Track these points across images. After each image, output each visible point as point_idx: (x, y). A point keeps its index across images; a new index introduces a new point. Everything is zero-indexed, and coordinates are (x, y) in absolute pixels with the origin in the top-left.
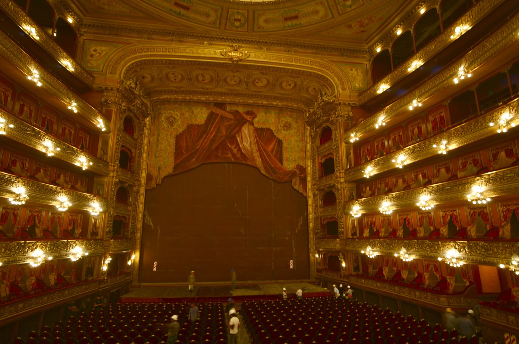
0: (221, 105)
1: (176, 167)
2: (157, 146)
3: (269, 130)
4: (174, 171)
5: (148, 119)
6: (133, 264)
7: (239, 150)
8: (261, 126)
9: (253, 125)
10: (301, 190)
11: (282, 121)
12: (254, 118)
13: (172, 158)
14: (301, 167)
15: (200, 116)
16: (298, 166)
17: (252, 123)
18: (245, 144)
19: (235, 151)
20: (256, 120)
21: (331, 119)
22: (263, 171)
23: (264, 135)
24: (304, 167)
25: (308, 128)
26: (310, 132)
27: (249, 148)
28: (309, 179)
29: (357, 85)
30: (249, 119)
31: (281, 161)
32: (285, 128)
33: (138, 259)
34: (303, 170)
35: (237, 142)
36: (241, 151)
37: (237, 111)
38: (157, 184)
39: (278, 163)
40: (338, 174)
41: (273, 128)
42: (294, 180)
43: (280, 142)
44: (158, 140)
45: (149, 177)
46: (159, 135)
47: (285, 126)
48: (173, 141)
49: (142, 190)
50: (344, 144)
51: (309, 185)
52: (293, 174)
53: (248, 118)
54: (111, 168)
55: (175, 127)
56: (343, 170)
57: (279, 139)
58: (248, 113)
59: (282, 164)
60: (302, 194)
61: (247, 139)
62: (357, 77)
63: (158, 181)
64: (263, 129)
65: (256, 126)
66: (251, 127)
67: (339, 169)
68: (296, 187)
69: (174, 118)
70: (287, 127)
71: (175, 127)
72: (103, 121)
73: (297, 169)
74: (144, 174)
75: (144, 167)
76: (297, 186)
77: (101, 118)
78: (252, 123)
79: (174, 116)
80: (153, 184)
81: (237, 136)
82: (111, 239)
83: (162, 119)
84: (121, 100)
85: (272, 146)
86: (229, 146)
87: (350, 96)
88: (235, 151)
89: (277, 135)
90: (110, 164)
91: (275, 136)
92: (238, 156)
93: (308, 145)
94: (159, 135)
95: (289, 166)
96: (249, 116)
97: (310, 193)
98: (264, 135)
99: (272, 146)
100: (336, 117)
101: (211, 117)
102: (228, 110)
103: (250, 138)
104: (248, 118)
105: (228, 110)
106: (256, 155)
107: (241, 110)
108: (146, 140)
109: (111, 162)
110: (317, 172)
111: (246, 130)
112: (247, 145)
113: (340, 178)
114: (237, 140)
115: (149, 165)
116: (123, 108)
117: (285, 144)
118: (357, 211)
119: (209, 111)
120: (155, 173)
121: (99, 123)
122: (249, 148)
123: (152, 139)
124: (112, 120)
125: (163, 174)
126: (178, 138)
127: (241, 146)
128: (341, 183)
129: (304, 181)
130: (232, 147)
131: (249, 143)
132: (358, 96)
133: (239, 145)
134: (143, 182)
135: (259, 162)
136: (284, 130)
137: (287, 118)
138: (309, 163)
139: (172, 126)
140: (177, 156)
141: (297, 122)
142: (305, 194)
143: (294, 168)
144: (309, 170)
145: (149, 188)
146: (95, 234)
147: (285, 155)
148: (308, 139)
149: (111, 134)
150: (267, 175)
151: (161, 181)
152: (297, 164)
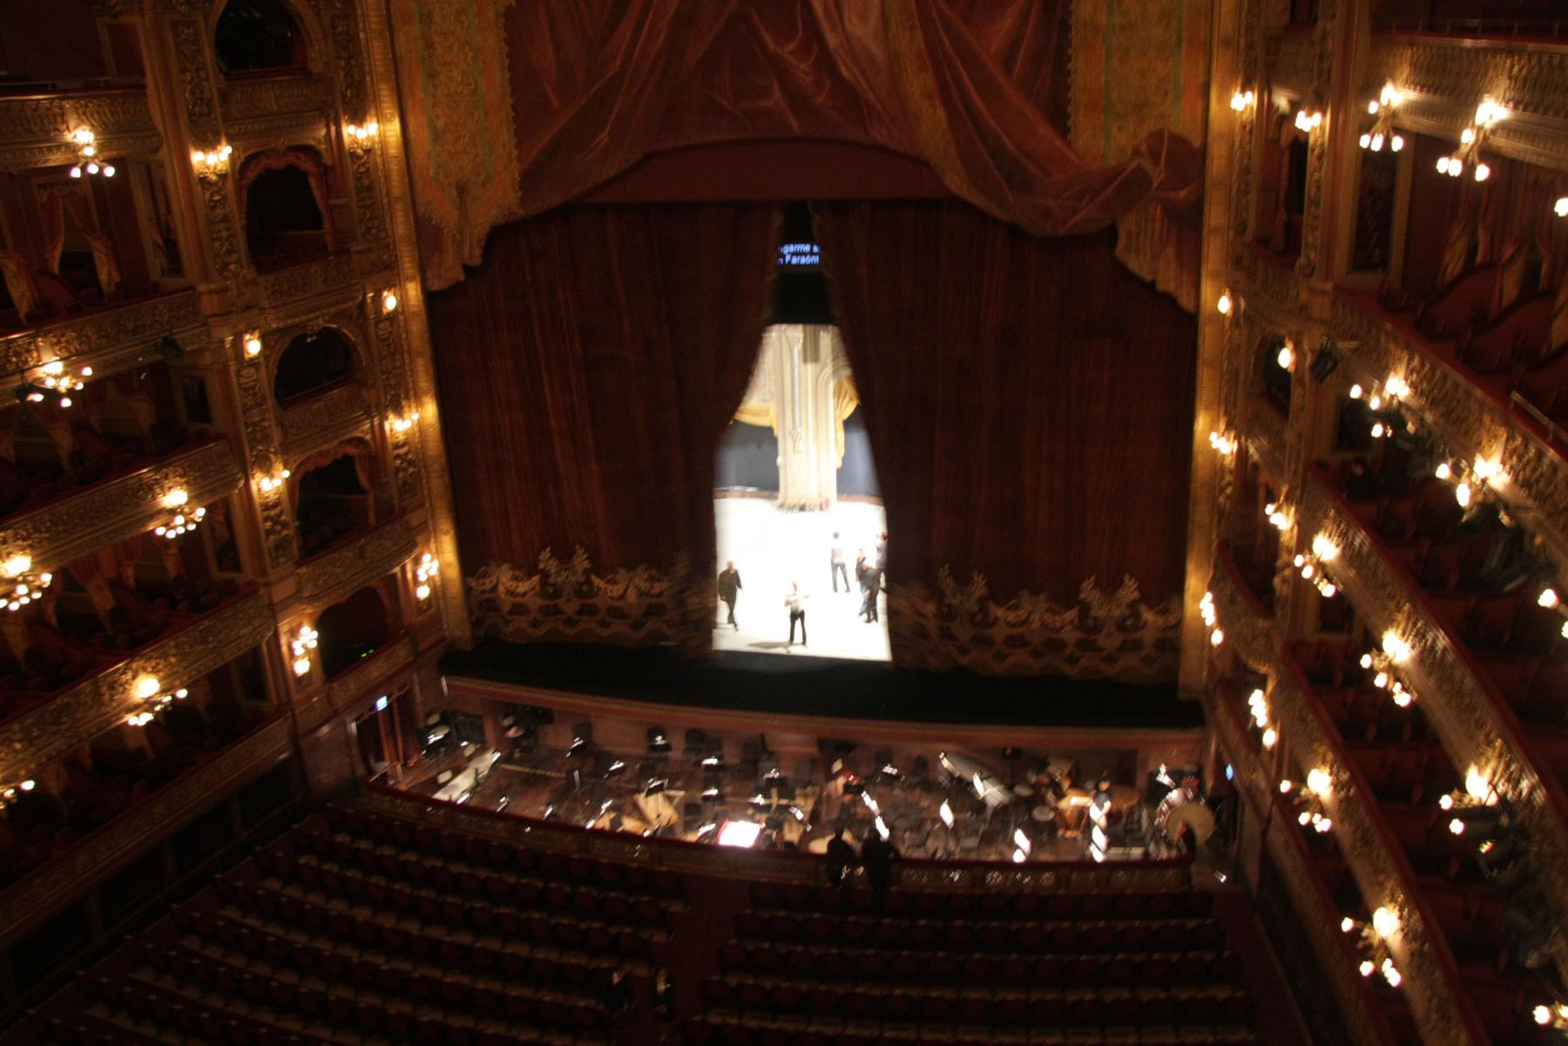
1: (529, 181)
2: (432, 75)
4: (523, 202)
6: (439, 589)
7: (825, 62)
10: (1168, 280)
13: (506, 137)
14: (1178, 141)
16: (1160, 133)
19: (803, 70)
22: (956, 182)
24: (1197, 143)
27: (878, 51)
28: (1215, 215)
31: (1059, 118)
33: (454, 573)
36: (833, 70)
38: (467, 269)
39: (1045, 130)
40: (1304, 296)
44: (430, 45)
45: (427, 237)
46: (427, 19)
48: (492, 42)
52: (1129, 187)
60: (1169, 300)
68: (1138, 264)
73: (1155, 156)
74: (401, 225)
75: (396, 192)
80: (450, 272)
85: (1005, 25)
86: (771, 44)
88: (803, 70)
90: (201, 288)
92: (819, 99)
94: (429, 15)
95: (1104, 141)
99: (1005, 25)
106: (918, 85)
109: (206, 279)
110: (1253, 196)
112: (862, 29)
115: (416, 176)
120: (444, 211)
122: (878, 51)
123: (401, 39)
125: (484, 217)
127: (832, 40)
129: (1186, 225)
131: (876, 12)
133: (819, 37)
135: (931, 127)
140: (524, 126)
142: (1185, 302)
143: (1136, 152)
145: (436, 285)
147: (1085, 72)
149: (164, 151)
150: (977, 199)
151: (478, 252)
152: (1151, 125)
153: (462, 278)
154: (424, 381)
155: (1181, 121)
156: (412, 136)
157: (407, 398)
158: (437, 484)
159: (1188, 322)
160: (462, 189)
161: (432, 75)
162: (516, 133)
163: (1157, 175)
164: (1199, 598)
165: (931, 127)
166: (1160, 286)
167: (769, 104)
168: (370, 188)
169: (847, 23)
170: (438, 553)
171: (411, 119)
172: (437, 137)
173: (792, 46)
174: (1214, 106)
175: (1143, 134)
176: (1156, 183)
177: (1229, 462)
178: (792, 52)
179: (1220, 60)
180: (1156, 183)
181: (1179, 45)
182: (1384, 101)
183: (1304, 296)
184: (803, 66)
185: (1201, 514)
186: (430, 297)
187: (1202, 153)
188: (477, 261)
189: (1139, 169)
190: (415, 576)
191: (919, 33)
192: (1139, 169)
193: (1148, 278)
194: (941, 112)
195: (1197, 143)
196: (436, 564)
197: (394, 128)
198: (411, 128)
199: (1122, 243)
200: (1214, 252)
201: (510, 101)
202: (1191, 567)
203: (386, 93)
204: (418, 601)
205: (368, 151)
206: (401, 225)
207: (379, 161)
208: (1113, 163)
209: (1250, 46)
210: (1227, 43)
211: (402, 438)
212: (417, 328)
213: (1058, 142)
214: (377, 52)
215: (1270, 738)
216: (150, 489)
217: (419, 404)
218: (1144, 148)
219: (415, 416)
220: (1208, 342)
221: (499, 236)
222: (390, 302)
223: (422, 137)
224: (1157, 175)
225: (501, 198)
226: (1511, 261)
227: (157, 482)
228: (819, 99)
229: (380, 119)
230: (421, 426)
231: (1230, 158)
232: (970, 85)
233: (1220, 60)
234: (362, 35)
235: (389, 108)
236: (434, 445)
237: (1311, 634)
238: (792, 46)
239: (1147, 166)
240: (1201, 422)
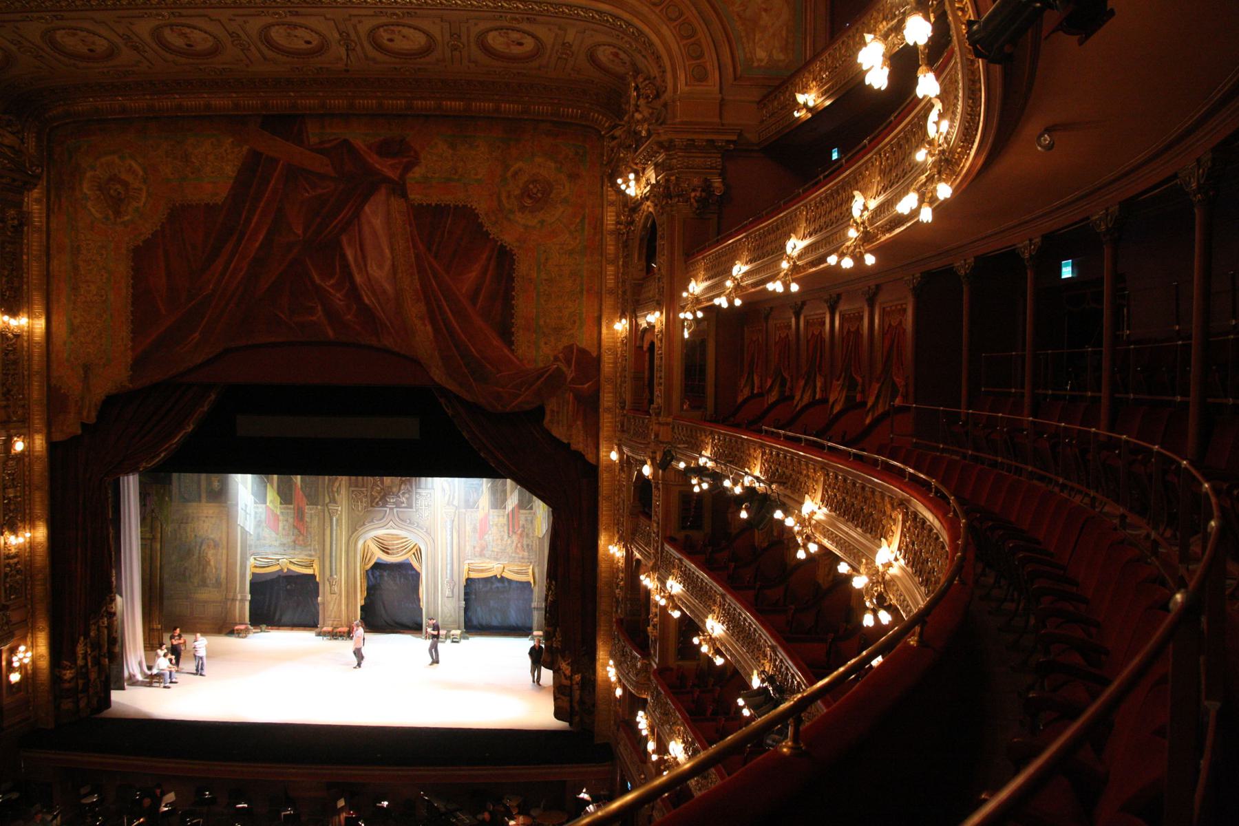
0: (285, 124)
2: (75, 289)
3: (466, 214)
7: (354, 293)
8: (434, 200)
10: (578, 443)
11: (515, 175)
12: (408, 168)
14: (582, 352)
15: (213, 169)
16: (569, 349)
17: (399, 189)
18: (374, 270)
19: (338, 299)
20: (417, 173)
22: (438, 375)
23: (446, 233)
24: (595, 355)
28: (607, 399)
29: (761, 54)
31: (506, 334)
32: (528, 202)
35: (345, 265)
36: (359, 299)
37: (345, 140)
38: (84, 426)
41: (481, 205)
42: (551, 405)
43: (504, 258)
44: (76, 268)
45: (56, 402)
47: (526, 193)
53: (386, 167)
55: (126, 218)
58: (384, 149)
59: (510, 344)
60: (580, 456)
61: (380, 251)
62: (765, 19)
63: (85, 414)
64: (440, 211)
65: (416, 197)
66: (397, 204)
68: (558, 432)
69: (125, 184)
70: (537, 196)
71: (126, 218)
73: (568, 362)
74: (36, 391)
75: (36, 368)
76: (562, 427)
78: (399, 189)
79: (124, 176)
80: (71, 426)
81: (344, 239)
83: (85, 190)
86: (317, 280)
87: (722, 103)
89: (494, 231)
91: (487, 234)
93: (611, 269)
95: (536, 351)
96: (391, 162)
101: (253, 171)
102: (314, 140)
103: (392, 250)
104: (386, 167)
105: (314, 140)
106: (415, 310)
107: (360, 137)
112: (379, 272)
114: (343, 257)
115: (53, 356)
117: (523, 267)
119: (245, 148)
122: (388, 287)
125: (103, 387)
126: (141, 256)
127: (358, 279)
129: (589, 407)
130: (328, 284)
131: (389, 263)
132: (761, 103)
133: (350, 276)
135: (423, 338)
136: (523, 208)
137: (538, 160)
139: (118, 213)
141: (573, 177)
142: (590, 458)
143: (556, 359)
145: (58, 437)
147: (523, 306)
150: (451, 386)
151: (94, 414)
152: (565, 341)
153: (80, 432)
154: (39, 509)
155: (584, 340)
156: (54, 329)
157: (23, 521)
158: (40, 589)
159: (592, 470)
160: (87, 368)
161: (75, 289)
162: (133, 332)
163: (570, 374)
164: (606, 665)
165: (423, 338)
166: (574, 447)
167: (314, 318)
168: (15, 362)
169: (369, 269)
170: (33, 646)
171: (54, 317)
172: (73, 331)
174: (604, 331)
175: (561, 348)
177: (622, 563)
178: (332, 286)
179: (608, 302)
181: (581, 292)
182: (691, 290)
183: (655, 427)
185: (603, 605)
186: (52, 446)
187: (598, 360)
188: (93, 419)
189: (558, 369)
192: (558, 369)
193: (565, 441)
194: (429, 328)
195: (595, 355)
197: (40, 325)
198: (54, 324)
199: (548, 418)
200: (607, 422)
201: (130, 308)
202: (600, 643)
203: (37, 298)
205: (17, 336)
207: (25, 344)
208: (541, 365)
209: (624, 293)
210: (611, 292)
211: (13, 551)
212: (39, 468)
213: (506, 351)
214: (35, 271)
217: (33, 527)
218: (561, 356)
219: (28, 535)
220: (605, 482)
221: (110, 403)
222: (19, 446)
223: (61, 330)
224: (570, 374)
225: (115, 375)
226: (771, 386)
229: (31, 315)
230: (32, 544)
231: (615, 363)
232: (450, 314)
233: (608, 302)
234: (25, 257)
235: (38, 308)
237: (673, 662)
239: (564, 369)
240: (602, 540)
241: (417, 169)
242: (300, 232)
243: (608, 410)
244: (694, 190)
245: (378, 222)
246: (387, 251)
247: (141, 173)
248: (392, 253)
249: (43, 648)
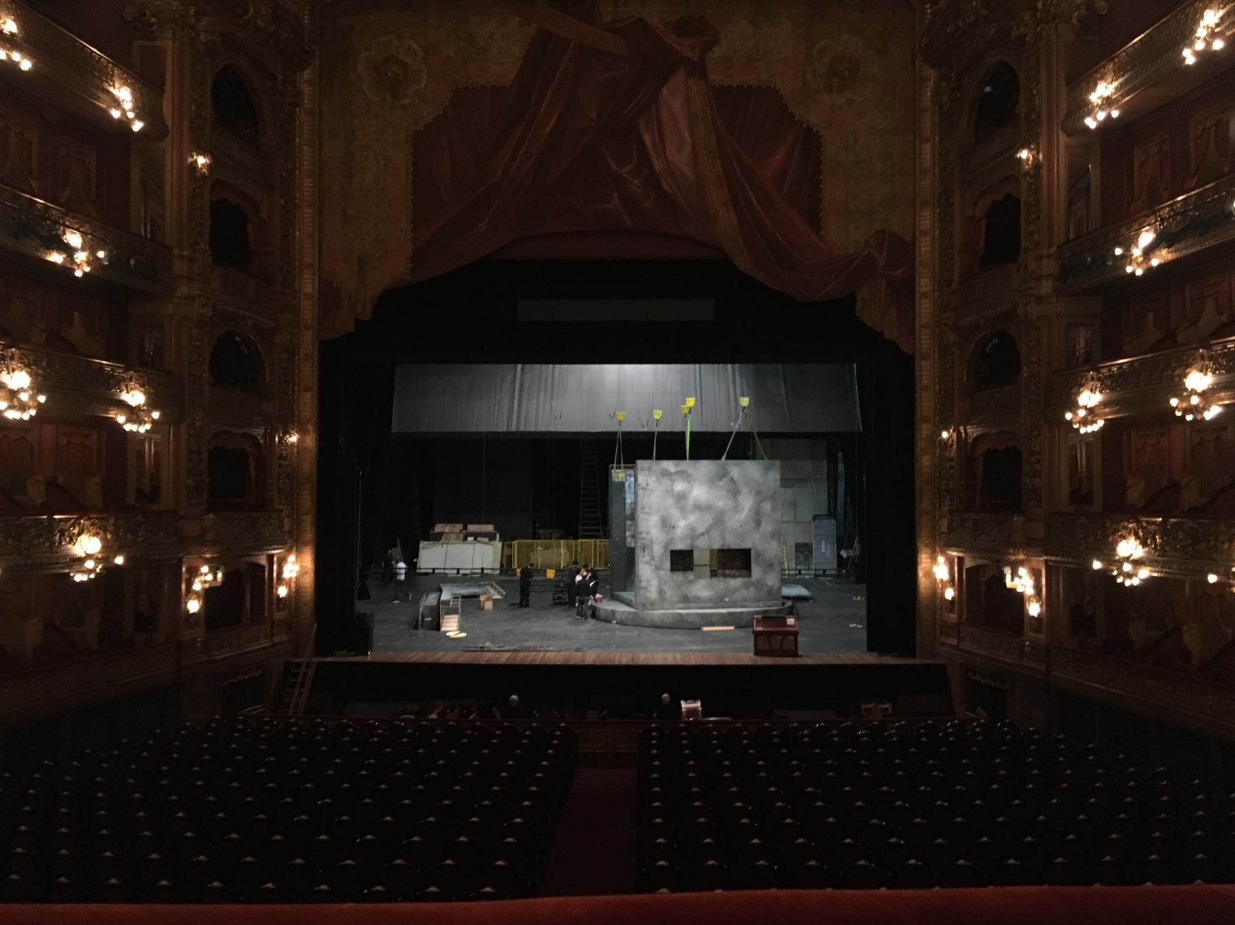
5: (307, 74)
6: (296, 593)
9: (704, 75)
17: (698, 70)
18: (672, 154)
20: (718, 52)
21: (1014, 34)
22: (743, 263)
23: (746, 114)
24: (908, 238)
25: (931, 73)
26: (937, 92)
27: (689, 173)
28: (924, 284)
30: (687, 53)
33: (309, 580)
34: (901, 250)
37: (642, 19)
40: (1032, 265)
43: (810, 141)
45: (328, 295)
49: (308, 343)
50: (1063, 139)
51: (925, 309)
54: (180, 267)
55: (406, 102)
56: (1050, 247)
57: (809, 129)
61: (679, 135)
67: (1037, 244)
71: (406, 102)
72: (134, 94)
74: (308, 285)
77: (125, 84)
78: (698, 70)
81: (642, 125)
82: (207, 512)
84: (192, 9)
86: (614, 168)
90: (176, 251)
95: (844, 235)
97: (925, 341)
98: (746, 114)
100: (1038, 25)
108: (306, 157)
111: (677, 100)
113: (1039, 279)
114: (641, 142)
116: (203, 37)
118: (1091, 411)
121: (117, 103)
122: (689, 173)
124: (168, 88)
127: (658, 166)
128: (1039, 299)
129: (904, 292)
133: (649, 160)
134: (308, 312)
138: (926, 218)
142: (904, 347)
144: (925, 249)
146: (151, 495)
148: (928, 125)
153: (352, 328)
166: (887, 336)
173: (629, 168)
176: (881, 265)
180: (881, 265)
184: (636, 181)
187: (912, 247)
190: (280, 572)
191: (719, 162)
194: (733, 215)
196: (297, 568)
199: (859, 305)
204: (279, 599)
206: (308, 285)
208: (852, 251)
215: (1034, 609)
216: (119, 383)
221: (389, 299)
227: (124, 379)
228: (646, 205)
236: (308, 466)
238: (629, 168)
241: (716, 49)
242: (594, 116)
243: (924, 295)
244: (1078, 8)
245: (677, 106)
246: (687, 135)
247: (421, 54)
248: (692, 137)
249: (308, 560)
